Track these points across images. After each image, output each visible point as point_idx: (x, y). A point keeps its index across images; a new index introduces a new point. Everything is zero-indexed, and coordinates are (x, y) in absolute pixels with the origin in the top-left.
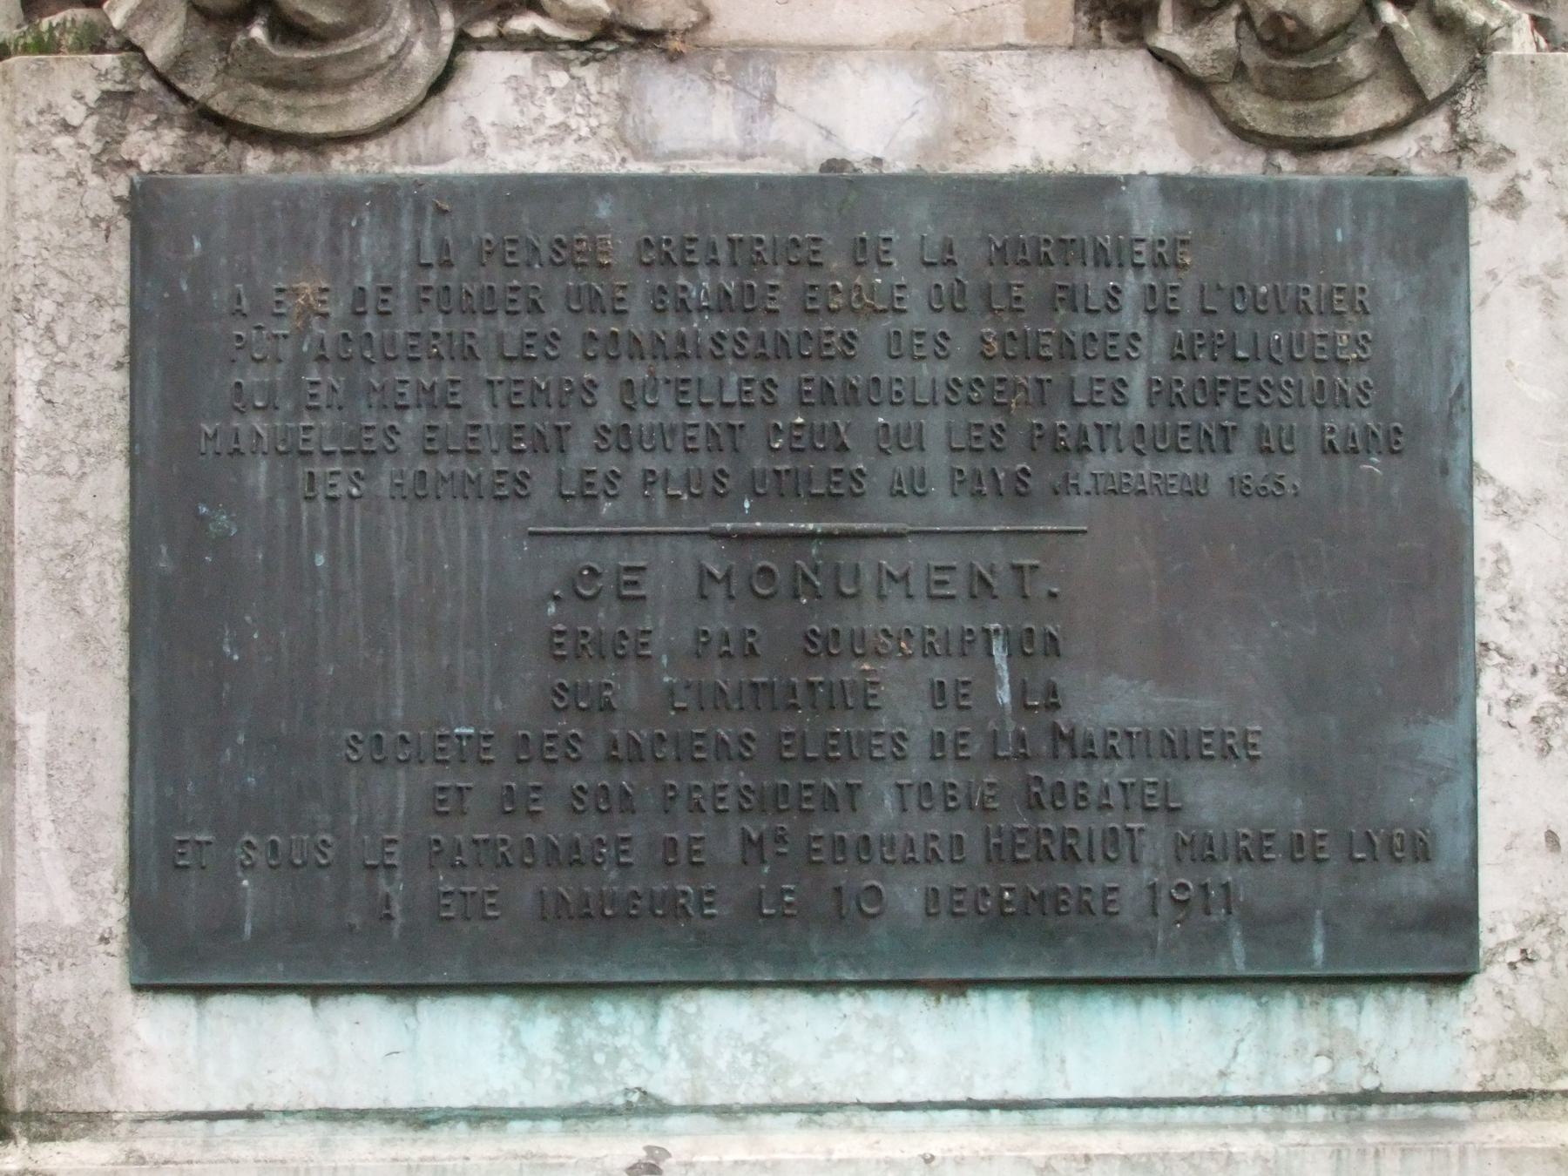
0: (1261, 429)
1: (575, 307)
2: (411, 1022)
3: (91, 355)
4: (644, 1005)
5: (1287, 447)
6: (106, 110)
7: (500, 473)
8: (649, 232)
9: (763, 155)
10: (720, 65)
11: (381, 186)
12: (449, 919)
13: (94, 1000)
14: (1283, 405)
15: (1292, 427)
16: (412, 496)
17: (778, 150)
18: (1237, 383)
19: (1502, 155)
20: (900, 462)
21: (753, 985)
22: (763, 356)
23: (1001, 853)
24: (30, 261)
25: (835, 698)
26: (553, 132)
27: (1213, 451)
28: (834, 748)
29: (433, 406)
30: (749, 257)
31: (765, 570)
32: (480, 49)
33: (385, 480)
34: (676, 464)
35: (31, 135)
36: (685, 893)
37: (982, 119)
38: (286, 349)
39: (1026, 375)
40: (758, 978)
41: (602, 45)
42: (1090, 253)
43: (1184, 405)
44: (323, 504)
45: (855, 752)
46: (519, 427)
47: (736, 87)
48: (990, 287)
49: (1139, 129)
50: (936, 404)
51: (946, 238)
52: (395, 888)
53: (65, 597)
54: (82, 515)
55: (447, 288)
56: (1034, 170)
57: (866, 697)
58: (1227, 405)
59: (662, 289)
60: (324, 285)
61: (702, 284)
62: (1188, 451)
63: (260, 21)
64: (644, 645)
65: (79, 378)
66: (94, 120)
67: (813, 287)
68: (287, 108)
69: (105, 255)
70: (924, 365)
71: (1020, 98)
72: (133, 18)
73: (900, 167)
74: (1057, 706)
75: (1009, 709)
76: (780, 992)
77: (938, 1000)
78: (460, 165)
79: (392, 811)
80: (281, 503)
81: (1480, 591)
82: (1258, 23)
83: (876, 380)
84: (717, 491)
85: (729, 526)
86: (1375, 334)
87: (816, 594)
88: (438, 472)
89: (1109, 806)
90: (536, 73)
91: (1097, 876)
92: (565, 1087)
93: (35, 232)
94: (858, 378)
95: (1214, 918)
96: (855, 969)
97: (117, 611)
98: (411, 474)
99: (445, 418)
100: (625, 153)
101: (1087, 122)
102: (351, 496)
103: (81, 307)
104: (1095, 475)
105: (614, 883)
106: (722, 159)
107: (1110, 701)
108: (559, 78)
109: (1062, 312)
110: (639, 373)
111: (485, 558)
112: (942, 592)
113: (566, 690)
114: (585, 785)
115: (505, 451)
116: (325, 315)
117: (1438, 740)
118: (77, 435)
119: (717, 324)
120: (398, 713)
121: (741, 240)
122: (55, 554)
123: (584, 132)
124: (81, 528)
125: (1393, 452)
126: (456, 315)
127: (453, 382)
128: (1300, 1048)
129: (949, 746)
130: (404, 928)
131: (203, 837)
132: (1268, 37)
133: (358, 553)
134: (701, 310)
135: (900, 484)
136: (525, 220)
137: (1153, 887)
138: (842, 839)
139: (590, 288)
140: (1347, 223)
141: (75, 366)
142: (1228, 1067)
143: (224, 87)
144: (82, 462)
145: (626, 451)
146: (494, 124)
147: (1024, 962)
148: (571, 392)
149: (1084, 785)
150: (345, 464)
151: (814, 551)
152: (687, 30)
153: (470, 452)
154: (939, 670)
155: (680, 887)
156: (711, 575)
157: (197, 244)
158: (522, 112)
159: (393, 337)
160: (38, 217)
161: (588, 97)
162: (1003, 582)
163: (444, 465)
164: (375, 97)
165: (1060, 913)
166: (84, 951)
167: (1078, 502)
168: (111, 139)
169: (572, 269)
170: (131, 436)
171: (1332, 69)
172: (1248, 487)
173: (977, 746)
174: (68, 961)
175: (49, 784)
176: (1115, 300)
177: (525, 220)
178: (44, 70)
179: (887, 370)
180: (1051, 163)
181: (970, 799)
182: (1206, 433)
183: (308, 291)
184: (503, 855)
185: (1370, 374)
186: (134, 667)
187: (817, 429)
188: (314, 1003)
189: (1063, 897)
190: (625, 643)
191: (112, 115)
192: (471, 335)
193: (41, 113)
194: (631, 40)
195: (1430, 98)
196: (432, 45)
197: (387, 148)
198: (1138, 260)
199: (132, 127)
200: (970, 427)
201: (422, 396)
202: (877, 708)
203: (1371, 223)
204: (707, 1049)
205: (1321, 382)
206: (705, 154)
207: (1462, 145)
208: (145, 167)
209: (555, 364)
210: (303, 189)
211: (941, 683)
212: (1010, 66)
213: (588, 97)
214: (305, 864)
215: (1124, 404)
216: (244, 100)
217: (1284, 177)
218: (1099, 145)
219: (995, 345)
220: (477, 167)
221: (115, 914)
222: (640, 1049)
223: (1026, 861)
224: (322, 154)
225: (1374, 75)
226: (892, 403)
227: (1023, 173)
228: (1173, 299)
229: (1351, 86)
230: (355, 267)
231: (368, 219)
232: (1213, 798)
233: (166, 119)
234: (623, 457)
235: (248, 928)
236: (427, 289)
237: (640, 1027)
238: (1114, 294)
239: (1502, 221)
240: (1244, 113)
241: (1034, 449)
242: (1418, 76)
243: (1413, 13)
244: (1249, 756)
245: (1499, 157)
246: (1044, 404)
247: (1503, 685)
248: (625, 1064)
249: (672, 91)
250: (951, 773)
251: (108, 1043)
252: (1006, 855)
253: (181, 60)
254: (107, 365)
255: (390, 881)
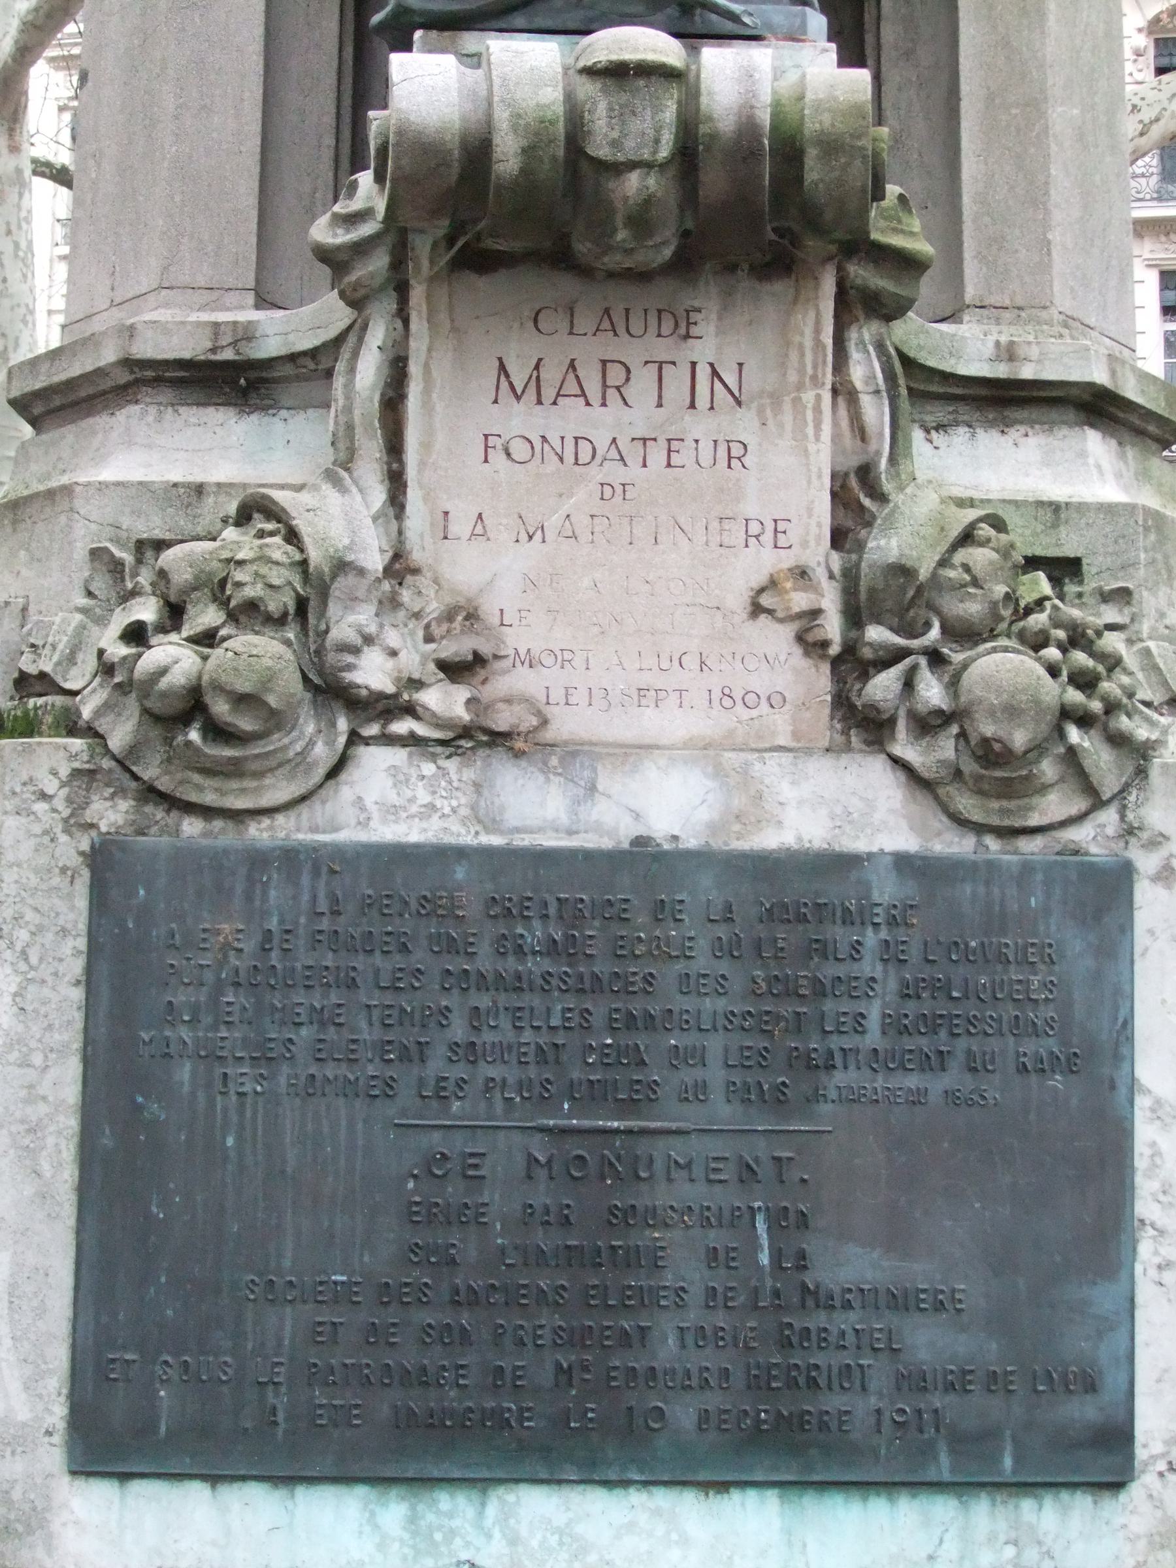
0: (969, 1052)
1: (436, 949)
2: (290, 1504)
3: (56, 974)
4: (475, 1495)
5: (990, 1067)
6: (75, 783)
7: (373, 1077)
8: (496, 892)
9: (586, 832)
10: (554, 761)
11: (288, 851)
12: (321, 1426)
13: (39, 1481)
14: (986, 1034)
15: (993, 1052)
16: (303, 1093)
17: (598, 828)
18: (952, 1017)
19: (1160, 839)
20: (689, 1076)
21: (560, 1482)
22: (582, 991)
23: (759, 1383)
24: (11, 899)
25: (631, 1260)
26: (422, 810)
27: (932, 1069)
28: (629, 1298)
29: (323, 1024)
30: (572, 914)
31: (580, 1158)
32: (367, 744)
33: (283, 1080)
34: (512, 1074)
35: (16, 801)
36: (509, 1410)
37: (756, 806)
38: (209, 976)
39: (787, 1009)
40: (566, 1477)
41: (462, 743)
42: (839, 914)
43: (910, 1034)
44: (234, 1098)
45: (646, 1301)
46: (389, 1042)
47: (566, 778)
48: (760, 938)
49: (878, 817)
50: (716, 1030)
51: (727, 901)
52: (280, 1401)
53: (28, 1162)
54: (44, 1098)
55: (336, 932)
56: (796, 847)
57: (657, 1258)
58: (943, 1034)
59: (504, 936)
60: (241, 927)
61: (535, 934)
62: (912, 1070)
63: (197, 725)
64: (483, 1214)
65: (46, 992)
66: (66, 790)
67: (622, 937)
68: (216, 790)
69: (70, 896)
70: (708, 1000)
71: (787, 791)
72: (98, 713)
73: (691, 842)
74: (805, 1267)
75: (768, 1269)
76: (581, 1487)
77: (707, 1494)
78: (349, 835)
79: (280, 1340)
80: (201, 1096)
81: (1139, 1179)
82: (973, 743)
83: (670, 1011)
84: (544, 1100)
85: (551, 1122)
86: (1059, 979)
87: (617, 1176)
88: (324, 1075)
89: (844, 1347)
90: (410, 764)
91: (834, 1402)
92: (410, 1558)
93: (16, 877)
94: (655, 1009)
95: (926, 1436)
96: (642, 1473)
97: (68, 1175)
98: (303, 1079)
99: (331, 1033)
100: (478, 828)
101: (839, 810)
102: (256, 1093)
103: (50, 936)
104: (839, 1088)
105: (453, 1400)
106: (555, 835)
107: (848, 1264)
108: (429, 768)
109: (816, 959)
110: (484, 1001)
111: (360, 1143)
112: (718, 1177)
113: (420, 1248)
114: (433, 1323)
115: (377, 1060)
116: (241, 950)
117: (1104, 1298)
118: (43, 1036)
119: (547, 965)
120: (287, 1263)
121: (567, 899)
122: (22, 1128)
123: (447, 810)
124: (43, 1108)
125: (1072, 1072)
126: (343, 953)
127: (339, 1005)
128: (992, 1538)
129: (720, 1298)
130: (286, 1431)
131: (128, 1357)
132: (980, 753)
133: (260, 1133)
134: (534, 953)
135: (686, 1092)
136: (399, 881)
137: (878, 1411)
138: (634, 1369)
139: (448, 934)
140: (1039, 893)
141: (43, 981)
142: (935, 1552)
143: (167, 772)
144: (46, 1057)
145: (472, 1062)
146: (377, 803)
147: (775, 1468)
148: (431, 1015)
149: (825, 1330)
150: (252, 1067)
151: (618, 1144)
152: (529, 732)
153: (350, 1060)
154: (716, 1238)
155: (505, 1405)
156: (536, 1160)
157: (142, 892)
158: (399, 794)
159: (293, 969)
160: (19, 866)
161: (450, 783)
162: (766, 1171)
163: (330, 1071)
164: (285, 783)
165: (804, 1430)
166: (33, 1442)
167: (825, 1108)
168: (78, 806)
169: (435, 920)
170: (85, 1037)
171: (1028, 778)
172: (959, 1098)
173: (742, 1298)
174: (19, 1449)
175: (10, 1308)
176: (858, 952)
177: (399, 881)
178: (28, 750)
179: (681, 1003)
180: (810, 842)
181: (735, 1338)
182: (927, 1055)
183: (227, 931)
184: (367, 1376)
185: (1056, 1011)
186: (80, 1220)
187: (623, 1048)
188: (213, 1487)
189: (807, 1418)
190: (467, 1212)
191: (79, 787)
192: (354, 969)
193: (24, 784)
194: (485, 738)
195: (1104, 798)
196: (330, 743)
197: (293, 819)
198: (876, 920)
199: (95, 798)
200: (742, 1048)
201: (315, 1015)
202: (663, 1267)
203: (1058, 892)
204: (524, 1533)
205: (1017, 1017)
206: (540, 830)
207: (1129, 831)
208: (104, 829)
209: (418, 993)
210: (226, 852)
211: (715, 1249)
212: (780, 765)
213: (450, 783)
214: (210, 1380)
215: (863, 1032)
216: (181, 782)
217: (990, 857)
218: (848, 828)
219: (763, 985)
220: (362, 836)
221: (58, 1413)
222: (469, 1529)
223: (778, 1389)
224: (242, 822)
225: (1062, 780)
226: (682, 1029)
227: (788, 849)
228: (903, 951)
229: (1044, 789)
230: (265, 914)
231: (275, 876)
232: (927, 1341)
233: (121, 792)
234: (470, 1066)
235: (163, 1429)
236: (320, 932)
237: (470, 1512)
238: (857, 946)
239: (1160, 891)
240: (961, 807)
241: (791, 1066)
242: (1095, 782)
243: (1092, 732)
244: (956, 1309)
245: (1157, 841)
246: (800, 1031)
247: (1156, 1253)
248: (458, 1541)
249: (516, 779)
250: (720, 1319)
251: (47, 1515)
252: (762, 1384)
253: (134, 750)
254: (69, 982)
255: (277, 1394)
